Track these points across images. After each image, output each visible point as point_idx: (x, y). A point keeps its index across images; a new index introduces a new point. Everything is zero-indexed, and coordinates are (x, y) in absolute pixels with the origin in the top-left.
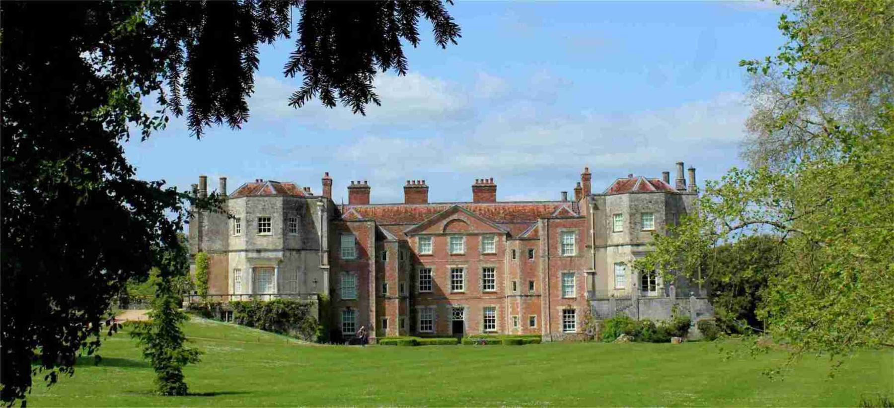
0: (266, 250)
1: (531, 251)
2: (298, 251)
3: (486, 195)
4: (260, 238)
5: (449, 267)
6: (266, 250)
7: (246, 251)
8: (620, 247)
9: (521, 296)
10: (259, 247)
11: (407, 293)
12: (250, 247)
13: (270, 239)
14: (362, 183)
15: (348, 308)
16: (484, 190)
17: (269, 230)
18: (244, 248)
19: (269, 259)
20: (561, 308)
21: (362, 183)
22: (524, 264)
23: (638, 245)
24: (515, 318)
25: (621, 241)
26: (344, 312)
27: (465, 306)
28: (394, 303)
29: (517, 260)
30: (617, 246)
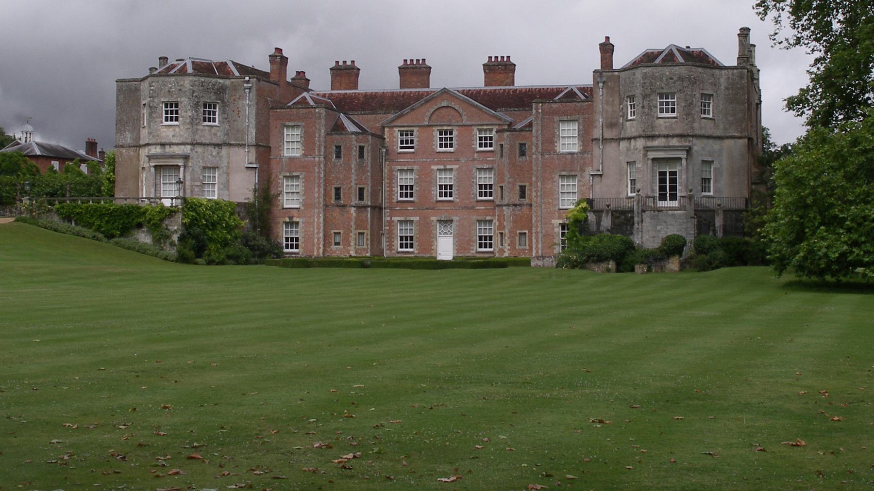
0: (171, 144)
1: (522, 145)
2: (218, 145)
3: (501, 77)
4: (165, 130)
5: (435, 167)
6: (171, 144)
11: (367, 201)
13: (177, 130)
14: (349, 63)
15: (291, 218)
16: (500, 68)
17: (177, 120)
19: (173, 156)
20: (557, 222)
21: (341, 63)
23: (653, 137)
24: (502, 234)
26: (287, 223)
27: (455, 218)
28: (348, 212)
29: (505, 160)
30: (629, 139)
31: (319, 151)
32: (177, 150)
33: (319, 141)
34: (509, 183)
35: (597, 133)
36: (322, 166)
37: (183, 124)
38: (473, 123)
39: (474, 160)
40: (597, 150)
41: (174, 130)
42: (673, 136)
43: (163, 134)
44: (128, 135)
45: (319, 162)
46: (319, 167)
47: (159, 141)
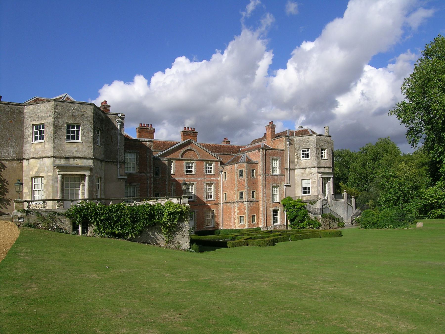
0: (74, 158)
4: (69, 145)
6: (74, 158)
7: (54, 157)
8: (307, 170)
9: (248, 202)
10: (67, 155)
12: (57, 154)
13: (80, 146)
18: (50, 154)
20: (272, 209)
22: (249, 180)
25: (308, 165)
31: (150, 169)
32: (80, 163)
33: (150, 163)
34: (248, 190)
35: (287, 165)
36: (152, 179)
37: (86, 143)
38: (203, 159)
39: (205, 179)
40: (287, 173)
41: (77, 147)
42: (326, 168)
43: (67, 149)
44: (11, 150)
45: (150, 177)
46: (150, 180)
47: (63, 154)
